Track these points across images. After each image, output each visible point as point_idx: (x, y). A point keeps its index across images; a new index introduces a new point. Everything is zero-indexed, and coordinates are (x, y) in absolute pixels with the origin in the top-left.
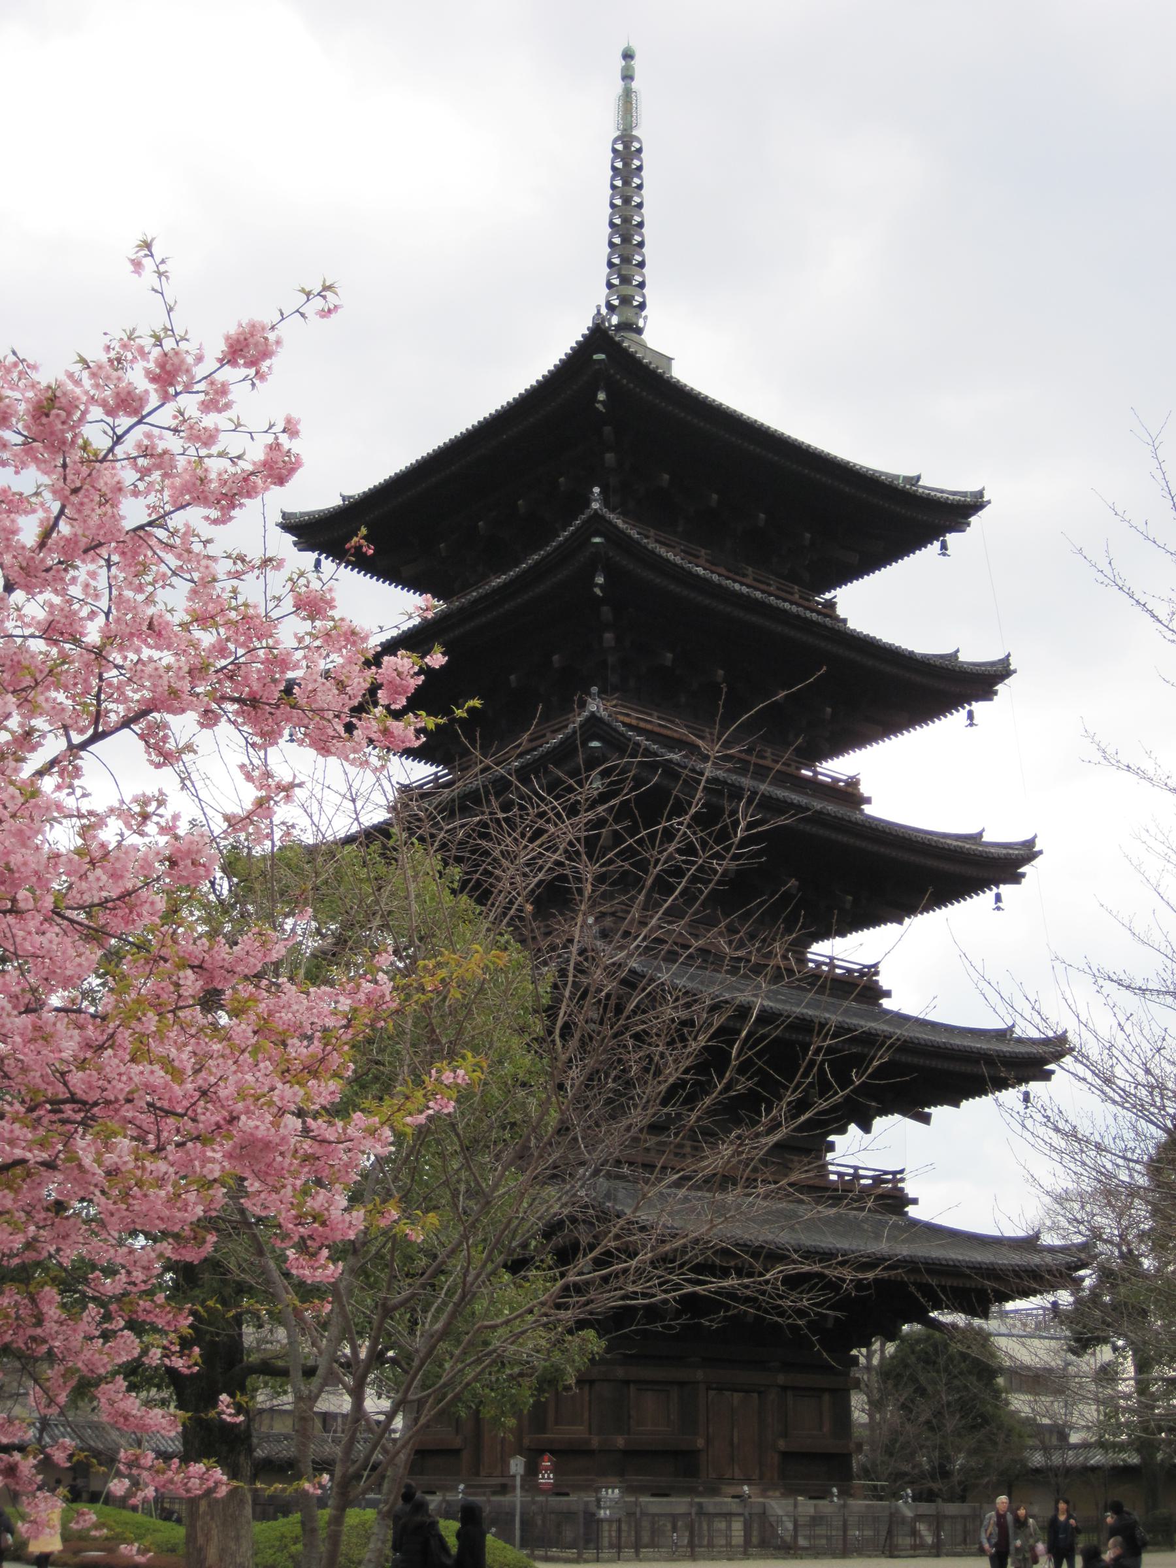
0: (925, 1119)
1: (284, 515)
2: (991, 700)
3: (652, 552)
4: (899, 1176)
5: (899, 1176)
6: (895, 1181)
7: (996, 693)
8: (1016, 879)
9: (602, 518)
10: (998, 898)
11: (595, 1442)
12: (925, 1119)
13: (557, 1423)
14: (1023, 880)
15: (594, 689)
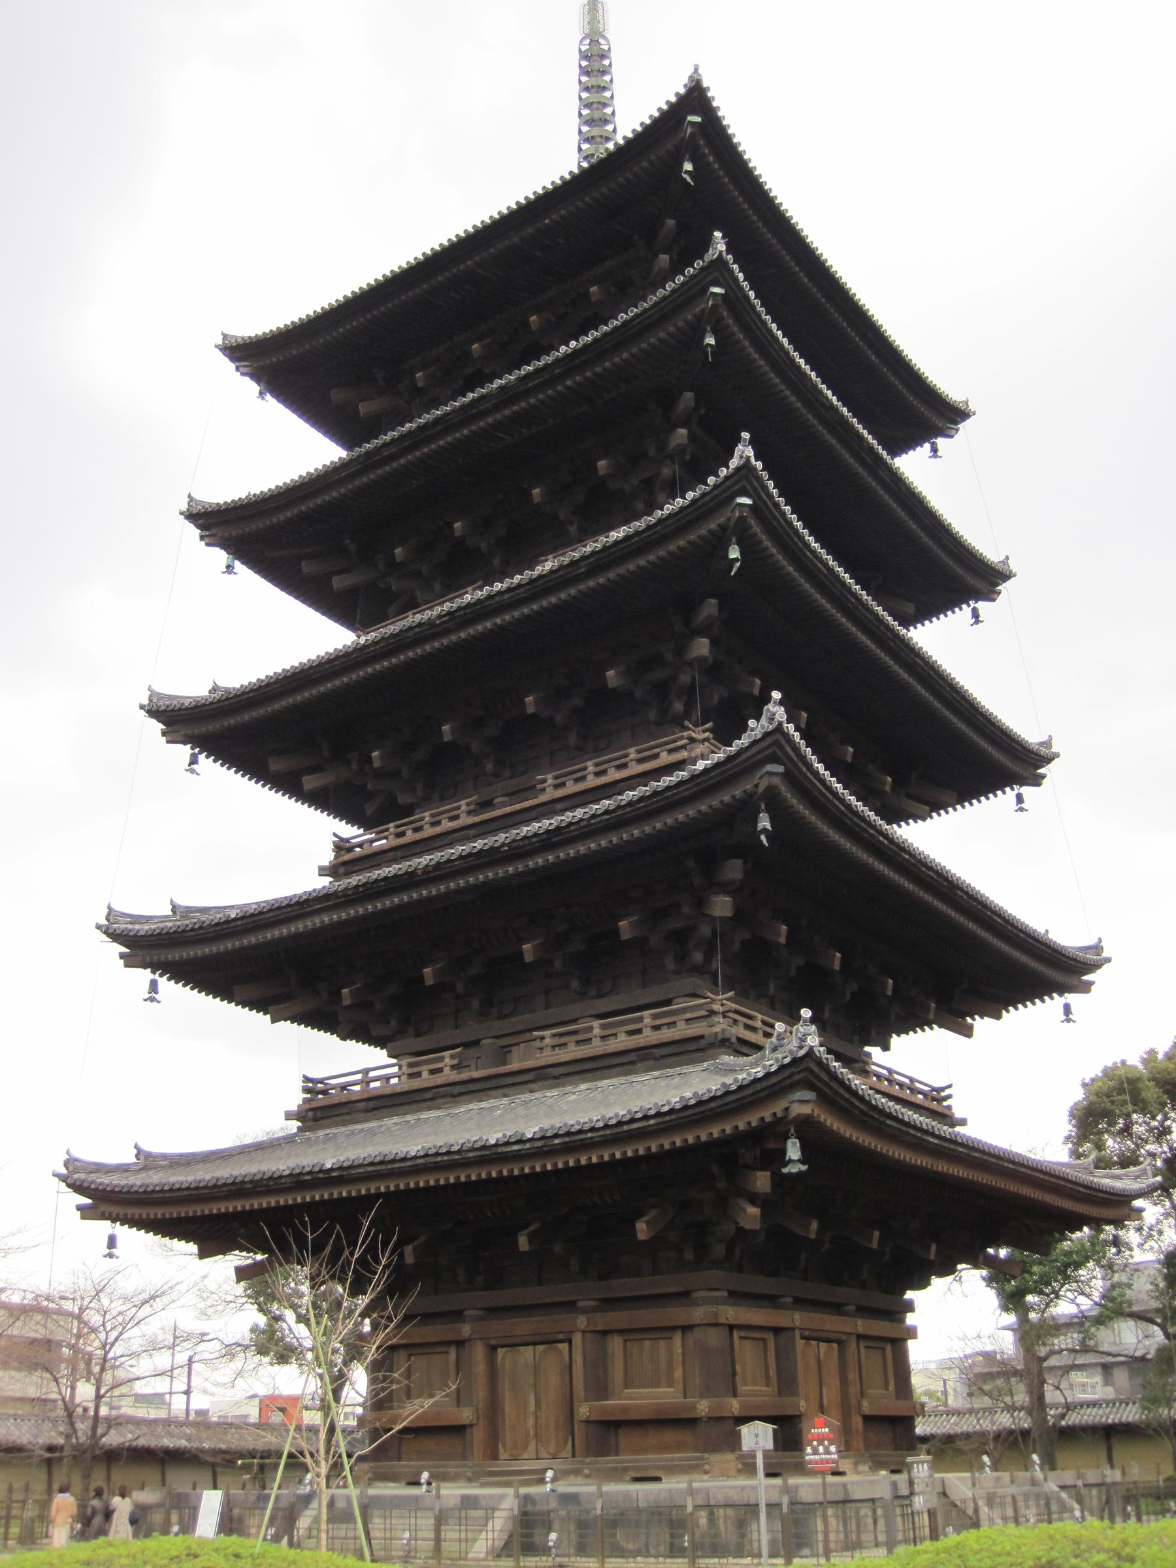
0: (967, 1032)
1: (225, 336)
2: (994, 600)
3: (764, 323)
4: (943, 1094)
5: (943, 1094)
6: (940, 1100)
7: (999, 593)
8: (1037, 781)
9: (726, 263)
10: (1020, 799)
11: (703, 1407)
12: (967, 1032)
13: (626, 1386)
14: (1044, 781)
15: (746, 435)
